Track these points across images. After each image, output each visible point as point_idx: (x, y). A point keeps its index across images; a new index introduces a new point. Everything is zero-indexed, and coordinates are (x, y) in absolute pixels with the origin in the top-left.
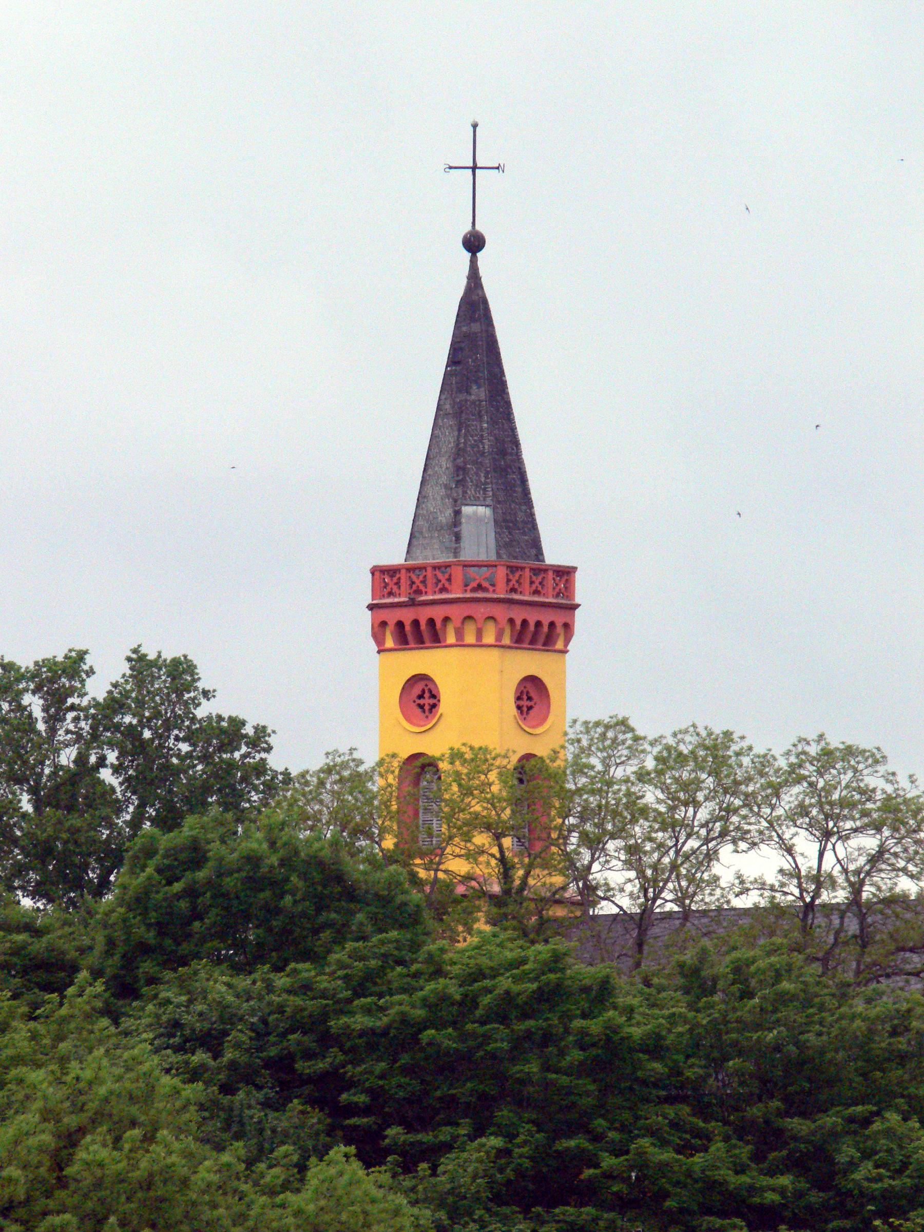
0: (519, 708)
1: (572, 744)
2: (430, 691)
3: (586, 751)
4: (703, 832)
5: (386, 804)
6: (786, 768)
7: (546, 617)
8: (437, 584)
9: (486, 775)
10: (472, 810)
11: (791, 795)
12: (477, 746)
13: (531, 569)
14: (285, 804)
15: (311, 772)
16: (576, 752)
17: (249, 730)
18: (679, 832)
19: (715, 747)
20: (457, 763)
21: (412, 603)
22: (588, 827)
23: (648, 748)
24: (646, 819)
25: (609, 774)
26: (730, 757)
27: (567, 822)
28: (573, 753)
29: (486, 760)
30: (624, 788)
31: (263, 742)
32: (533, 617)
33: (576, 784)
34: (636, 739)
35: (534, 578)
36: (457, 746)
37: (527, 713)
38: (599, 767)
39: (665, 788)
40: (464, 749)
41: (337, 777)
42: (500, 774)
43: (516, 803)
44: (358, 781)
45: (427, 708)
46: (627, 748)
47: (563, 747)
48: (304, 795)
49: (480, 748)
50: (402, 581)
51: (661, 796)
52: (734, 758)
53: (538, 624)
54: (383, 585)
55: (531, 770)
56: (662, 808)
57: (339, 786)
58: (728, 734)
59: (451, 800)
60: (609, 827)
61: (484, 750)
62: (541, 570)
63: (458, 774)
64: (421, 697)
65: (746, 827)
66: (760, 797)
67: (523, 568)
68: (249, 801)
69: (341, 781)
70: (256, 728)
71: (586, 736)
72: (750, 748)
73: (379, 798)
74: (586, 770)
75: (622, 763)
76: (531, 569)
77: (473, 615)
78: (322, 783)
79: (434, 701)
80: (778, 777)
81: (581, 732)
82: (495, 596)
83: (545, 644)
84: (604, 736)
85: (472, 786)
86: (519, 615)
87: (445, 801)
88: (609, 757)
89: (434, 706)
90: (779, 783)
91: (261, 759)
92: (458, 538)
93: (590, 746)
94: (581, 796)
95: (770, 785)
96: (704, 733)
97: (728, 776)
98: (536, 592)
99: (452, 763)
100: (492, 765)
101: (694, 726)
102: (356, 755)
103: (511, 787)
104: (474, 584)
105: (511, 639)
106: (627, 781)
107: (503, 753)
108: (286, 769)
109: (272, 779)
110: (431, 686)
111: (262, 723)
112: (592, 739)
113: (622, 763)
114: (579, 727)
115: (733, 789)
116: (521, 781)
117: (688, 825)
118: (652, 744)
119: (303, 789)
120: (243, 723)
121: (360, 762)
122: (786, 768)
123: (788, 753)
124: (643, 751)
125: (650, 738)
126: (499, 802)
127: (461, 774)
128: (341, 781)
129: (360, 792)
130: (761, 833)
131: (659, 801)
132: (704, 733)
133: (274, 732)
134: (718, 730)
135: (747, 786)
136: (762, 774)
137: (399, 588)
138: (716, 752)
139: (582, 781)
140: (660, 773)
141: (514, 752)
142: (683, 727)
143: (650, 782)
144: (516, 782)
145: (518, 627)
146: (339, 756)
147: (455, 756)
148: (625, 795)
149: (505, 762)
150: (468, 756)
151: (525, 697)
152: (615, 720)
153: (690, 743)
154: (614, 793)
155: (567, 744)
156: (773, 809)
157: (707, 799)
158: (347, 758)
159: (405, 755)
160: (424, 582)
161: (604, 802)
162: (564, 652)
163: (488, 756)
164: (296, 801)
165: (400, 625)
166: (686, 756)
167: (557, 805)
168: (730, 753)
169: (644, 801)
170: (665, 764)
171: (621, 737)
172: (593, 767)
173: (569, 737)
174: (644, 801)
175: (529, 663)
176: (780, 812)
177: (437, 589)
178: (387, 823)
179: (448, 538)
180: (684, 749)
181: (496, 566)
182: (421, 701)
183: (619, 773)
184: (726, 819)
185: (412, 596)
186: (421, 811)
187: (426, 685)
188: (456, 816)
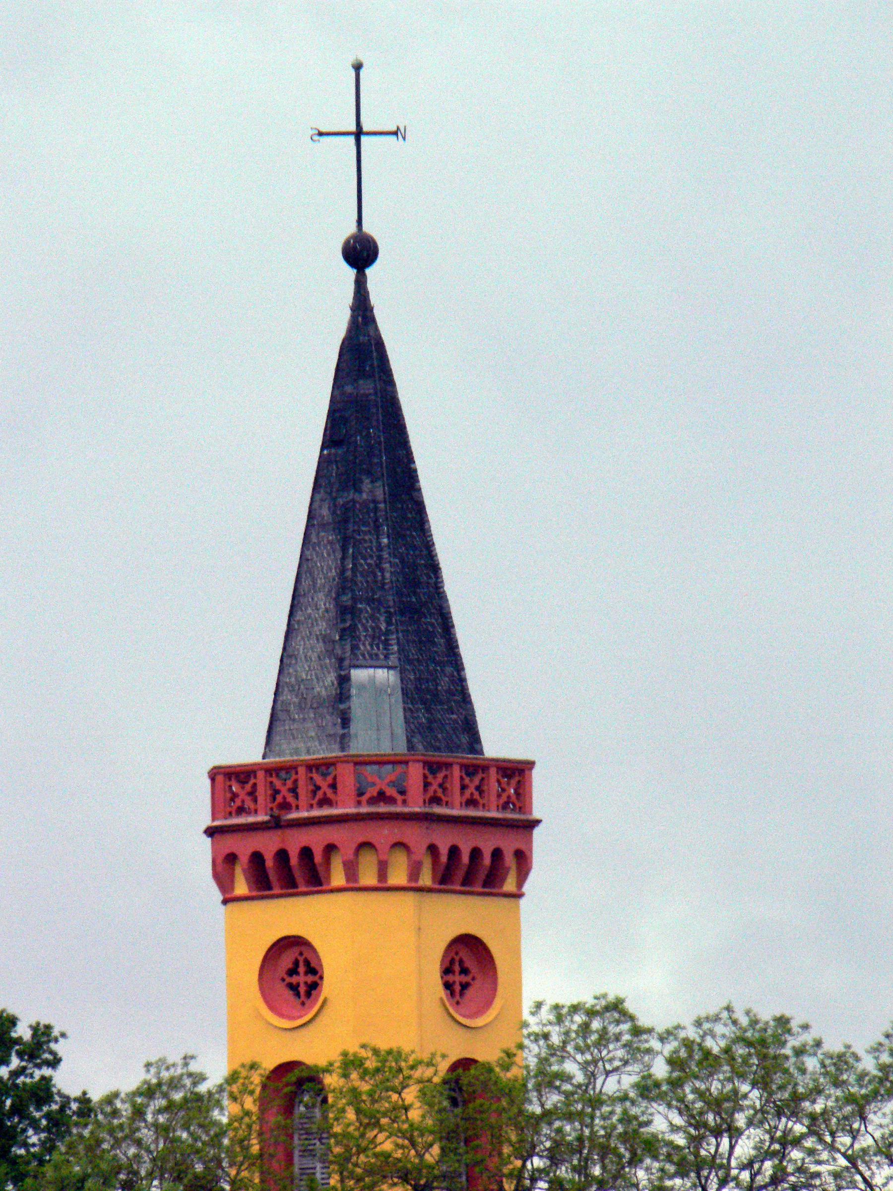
0: (448, 986)
1: (536, 1041)
2: (307, 962)
3: (559, 1052)
4: (745, 1176)
5: (243, 1143)
6: (875, 1072)
7: (487, 843)
8: (314, 793)
9: (400, 1094)
10: (378, 1149)
11: (884, 1115)
12: (383, 1046)
13: (463, 766)
14: (81, 1148)
15: (123, 1095)
16: (543, 1055)
17: (23, 1031)
18: (707, 1178)
19: (763, 1043)
20: (354, 1075)
21: (276, 824)
22: (563, 1172)
23: (655, 1044)
24: (655, 1158)
25: (594, 1089)
26: (787, 1058)
27: (529, 1166)
28: (538, 1056)
29: (400, 1070)
30: (619, 1110)
31: (44, 1052)
32: (466, 843)
33: (542, 1105)
34: (637, 1031)
35: (467, 780)
36: (353, 1048)
37: (462, 994)
38: (580, 1078)
39: (684, 1109)
40: (363, 1053)
41: (164, 1102)
42: (423, 1093)
43: (449, 1137)
44: (198, 1105)
45: (302, 989)
46: (625, 1046)
47: (521, 1047)
48: (111, 1132)
49: (390, 1052)
50: (301, 783)
51: (678, 1121)
52: (793, 1060)
53: (476, 853)
54: (229, 795)
55: (470, 1084)
56: (680, 1140)
57: (166, 1116)
58: (783, 1022)
59: (345, 1135)
60: (597, 1171)
61: (396, 1054)
62: (478, 768)
63: (355, 1092)
64: (293, 973)
65: (814, 1168)
66: (834, 1120)
67: (448, 765)
68: (25, 1145)
69: (170, 1107)
70: (35, 1029)
71: (557, 1028)
72: (818, 1044)
73: (231, 1134)
74: (558, 1083)
75: (616, 1070)
76: (463, 766)
77: (374, 841)
78: (139, 1113)
79: (316, 978)
80: (861, 1087)
81: (551, 1023)
82: (406, 810)
83: (486, 884)
84: (585, 1028)
85: (378, 1111)
86: (444, 840)
87: (335, 1136)
88: (595, 1062)
89: (314, 987)
90: (865, 1097)
91: (43, 1078)
92: (346, 721)
93: (565, 1043)
94: (550, 1124)
95: (850, 1099)
96: (744, 1021)
97: (781, 1088)
98: (471, 803)
99: (346, 1076)
100: (410, 1077)
101: (728, 1009)
102: (194, 1067)
103: (440, 1111)
104: (372, 792)
105: (434, 878)
106: (624, 1098)
107: (426, 1057)
108: (84, 1093)
109: (62, 1109)
110: (307, 954)
111: (44, 1021)
112: (567, 1033)
113: (616, 1070)
114: (546, 1014)
115: (791, 1107)
116: (454, 1102)
117: (721, 1166)
118: (662, 1039)
119: (110, 1123)
120: (13, 1021)
121: (199, 1078)
122: (875, 1072)
123: (877, 1049)
124: (649, 1051)
125: (660, 1029)
126: (422, 1135)
127: (360, 1093)
128: (170, 1107)
129: (201, 1126)
130: (836, 1175)
131: (674, 1129)
132: (744, 1021)
133: (63, 1035)
134: (766, 1015)
135: (814, 1102)
136: (837, 1084)
137: (255, 800)
138: (763, 1051)
139: (553, 1099)
140: (675, 1084)
141: (444, 1056)
142: (712, 1011)
143: (661, 1097)
144: (446, 1103)
145: (444, 859)
146: (168, 1069)
147: (350, 1063)
148: (620, 1121)
149: (429, 1072)
150: (371, 1064)
151: (457, 968)
152: (604, 1003)
153: (724, 1036)
154: (604, 1118)
155: (526, 1042)
156: (854, 1138)
157: (750, 1123)
158: (179, 1071)
159: (269, 1063)
160: (294, 790)
161: (587, 1132)
162: (519, 895)
163: (403, 1064)
164: (99, 1142)
165: (257, 858)
166: (717, 1057)
167: (514, 1138)
168: (787, 1051)
169: (651, 1129)
170: (683, 1070)
171: (613, 1029)
172: (568, 1078)
173: (530, 1030)
174: (651, 1129)
175: (462, 914)
176: (866, 1142)
177: (315, 802)
178: (245, 1174)
179: (331, 721)
180: (715, 1046)
181: (406, 763)
182: (294, 980)
183: (611, 1086)
184: (782, 1155)
185: (276, 812)
186: (296, 1154)
187: (301, 954)
188: (354, 1159)
